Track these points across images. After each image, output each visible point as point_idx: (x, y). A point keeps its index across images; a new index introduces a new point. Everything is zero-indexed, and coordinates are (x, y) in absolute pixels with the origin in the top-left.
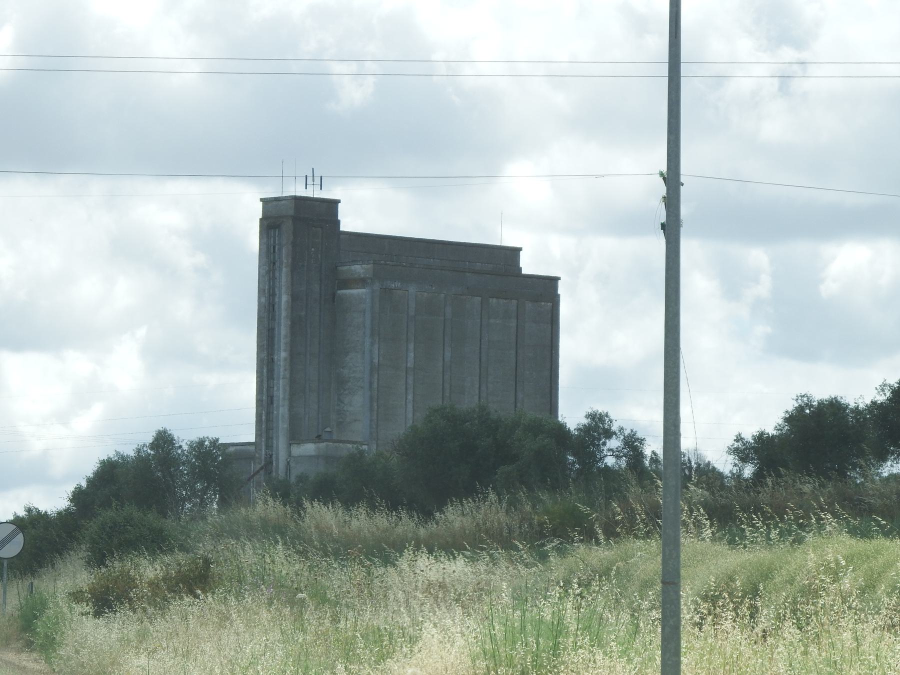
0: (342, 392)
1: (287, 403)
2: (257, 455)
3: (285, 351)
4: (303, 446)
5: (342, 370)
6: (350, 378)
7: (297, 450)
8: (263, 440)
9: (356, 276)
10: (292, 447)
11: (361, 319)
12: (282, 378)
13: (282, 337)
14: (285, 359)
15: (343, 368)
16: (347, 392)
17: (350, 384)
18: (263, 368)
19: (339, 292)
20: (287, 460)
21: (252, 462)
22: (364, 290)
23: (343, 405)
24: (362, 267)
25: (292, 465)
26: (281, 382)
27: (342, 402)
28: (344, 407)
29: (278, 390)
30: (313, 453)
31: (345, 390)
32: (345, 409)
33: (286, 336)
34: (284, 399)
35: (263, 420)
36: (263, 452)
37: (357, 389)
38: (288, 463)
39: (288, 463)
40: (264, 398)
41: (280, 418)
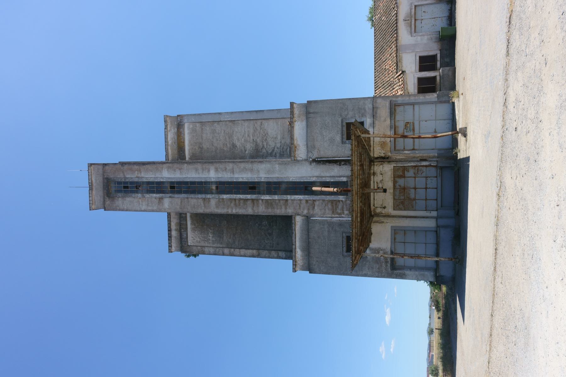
0: (264, 151)
1: (256, 166)
2: (305, 212)
3: (209, 171)
4: (297, 142)
5: (247, 152)
6: (253, 140)
7: (301, 153)
8: (289, 197)
9: (176, 138)
10: (299, 159)
11: (208, 129)
12: (233, 174)
13: (197, 176)
14: (217, 170)
15: (245, 151)
16: (265, 144)
17: (258, 140)
18: (223, 199)
19: (187, 159)
20: (311, 163)
21: (311, 218)
22: (186, 126)
23: (276, 149)
24: (169, 131)
25: (315, 155)
26: (236, 176)
27: (273, 150)
28: (277, 148)
29: (242, 178)
30: (304, 123)
31: (263, 147)
32: (278, 145)
33: (197, 170)
34: (252, 170)
35: (269, 198)
36: (301, 197)
37: (263, 130)
38: (314, 161)
39: (314, 161)
40: (249, 197)
41: (270, 176)
